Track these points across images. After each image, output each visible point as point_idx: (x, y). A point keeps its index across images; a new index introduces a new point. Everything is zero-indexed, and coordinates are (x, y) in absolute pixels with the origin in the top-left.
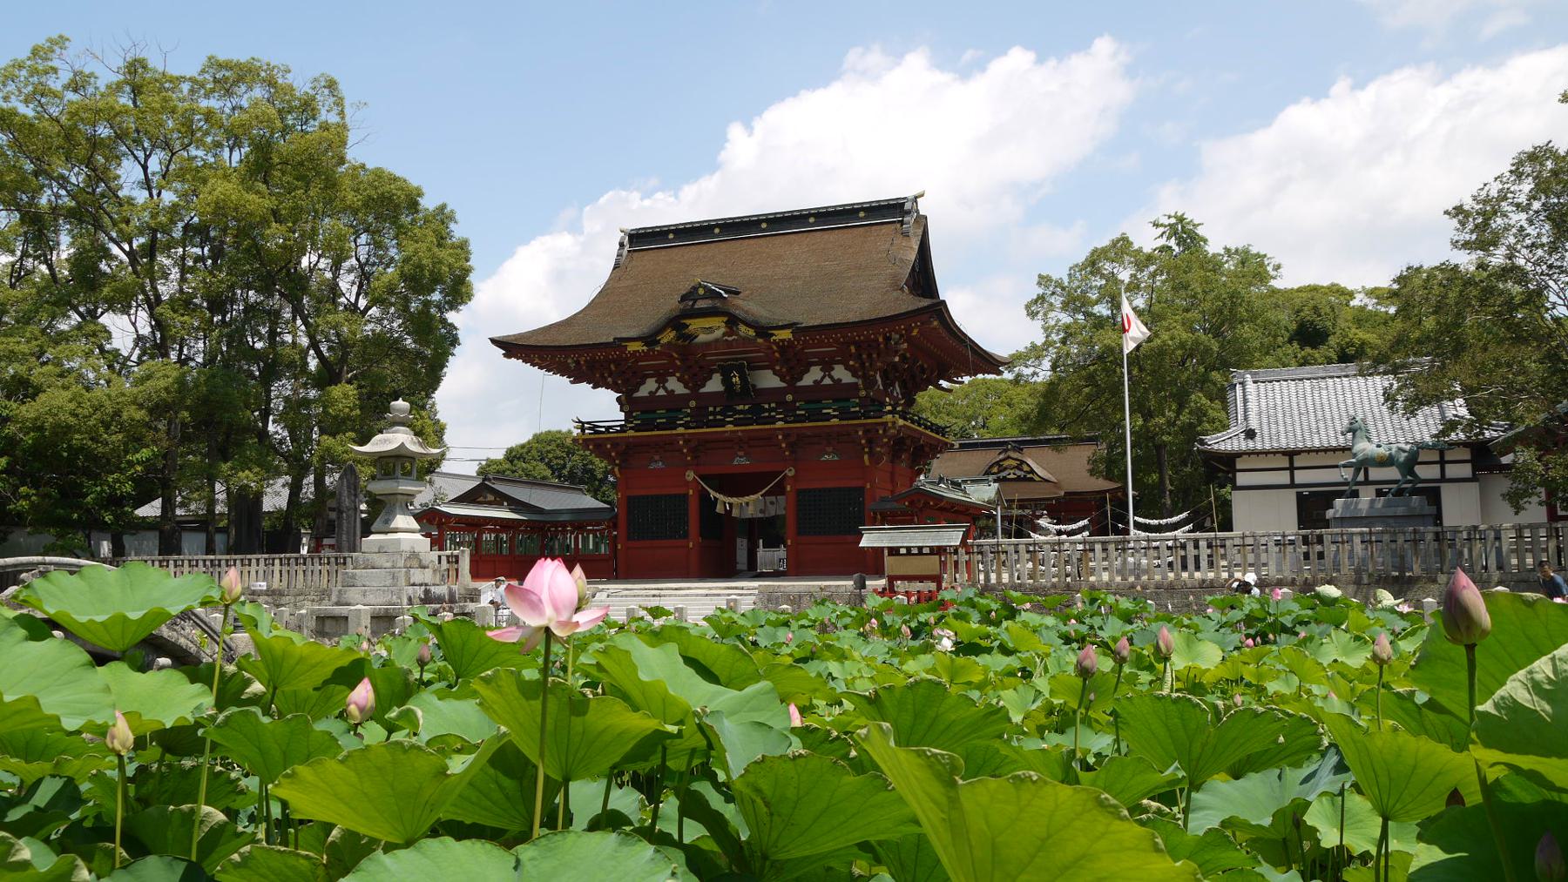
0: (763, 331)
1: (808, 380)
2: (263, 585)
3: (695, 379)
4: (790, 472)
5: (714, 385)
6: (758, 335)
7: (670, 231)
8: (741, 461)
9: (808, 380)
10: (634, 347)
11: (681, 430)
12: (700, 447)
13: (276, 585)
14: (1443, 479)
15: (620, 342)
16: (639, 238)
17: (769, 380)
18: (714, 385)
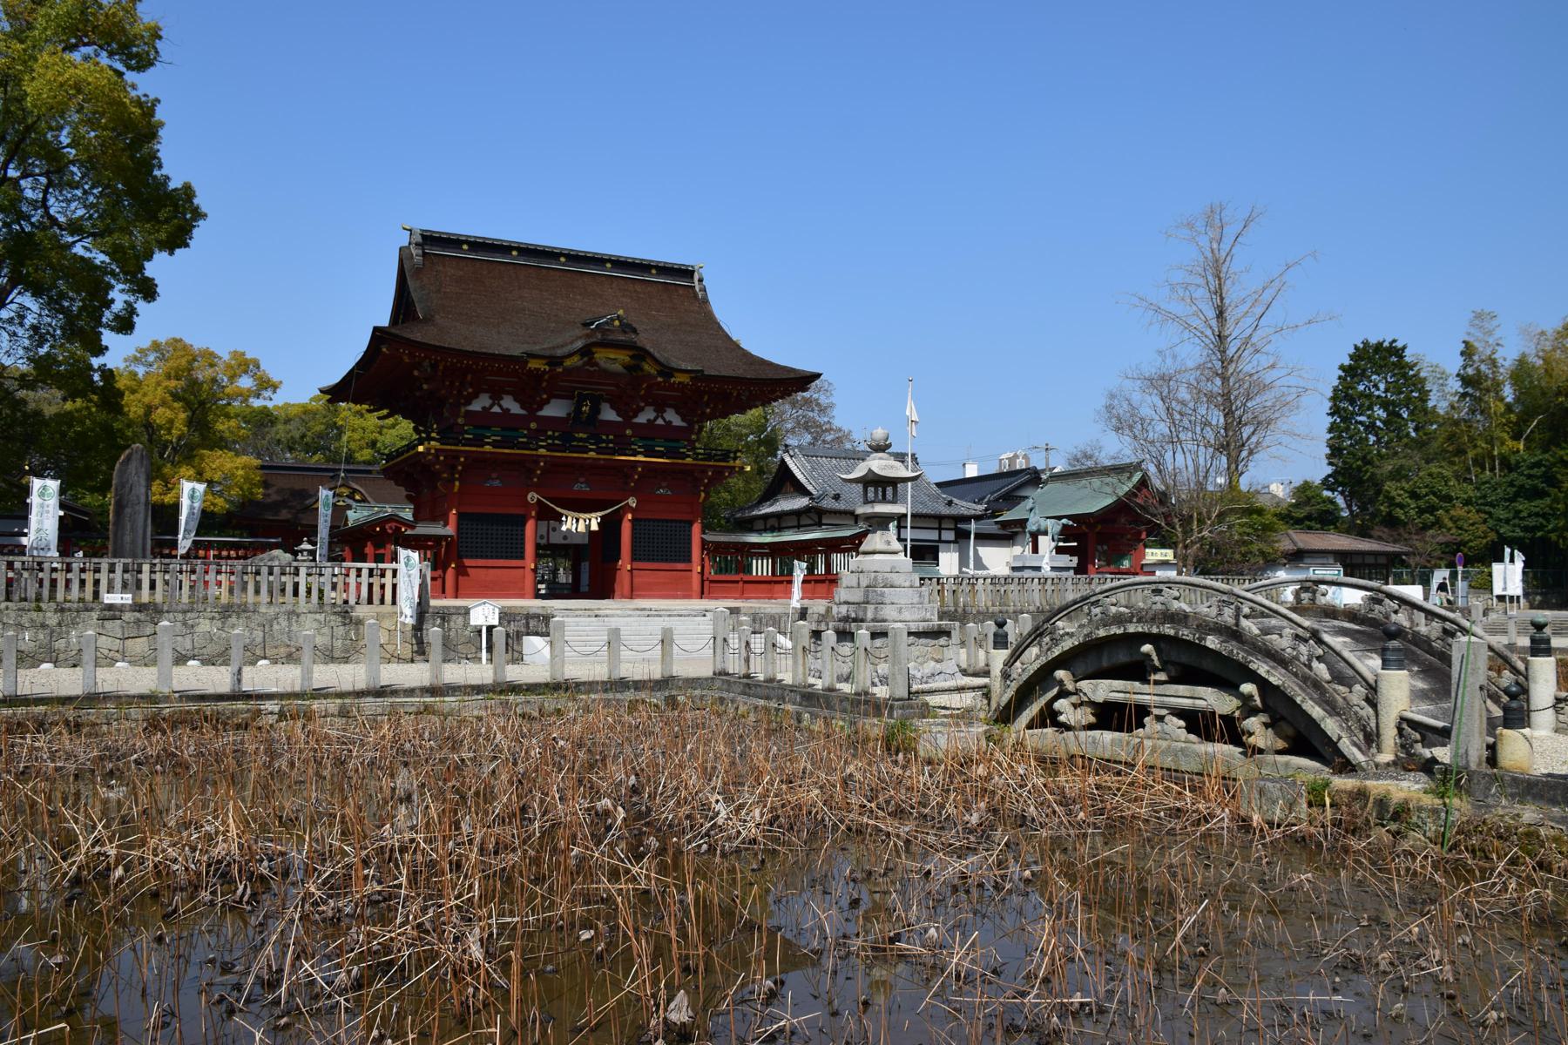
0: (667, 371)
1: (642, 419)
2: (127, 599)
3: (533, 404)
4: (632, 502)
5: (555, 410)
6: (660, 373)
7: (466, 242)
8: (581, 487)
9: (642, 419)
10: (533, 364)
11: (542, 451)
12: (555, 467)
13: (145, 596)
14: (940, 541)
15: (520, 361)
16: (430, 239)
17: (609, 414)
18: (555, 410)
